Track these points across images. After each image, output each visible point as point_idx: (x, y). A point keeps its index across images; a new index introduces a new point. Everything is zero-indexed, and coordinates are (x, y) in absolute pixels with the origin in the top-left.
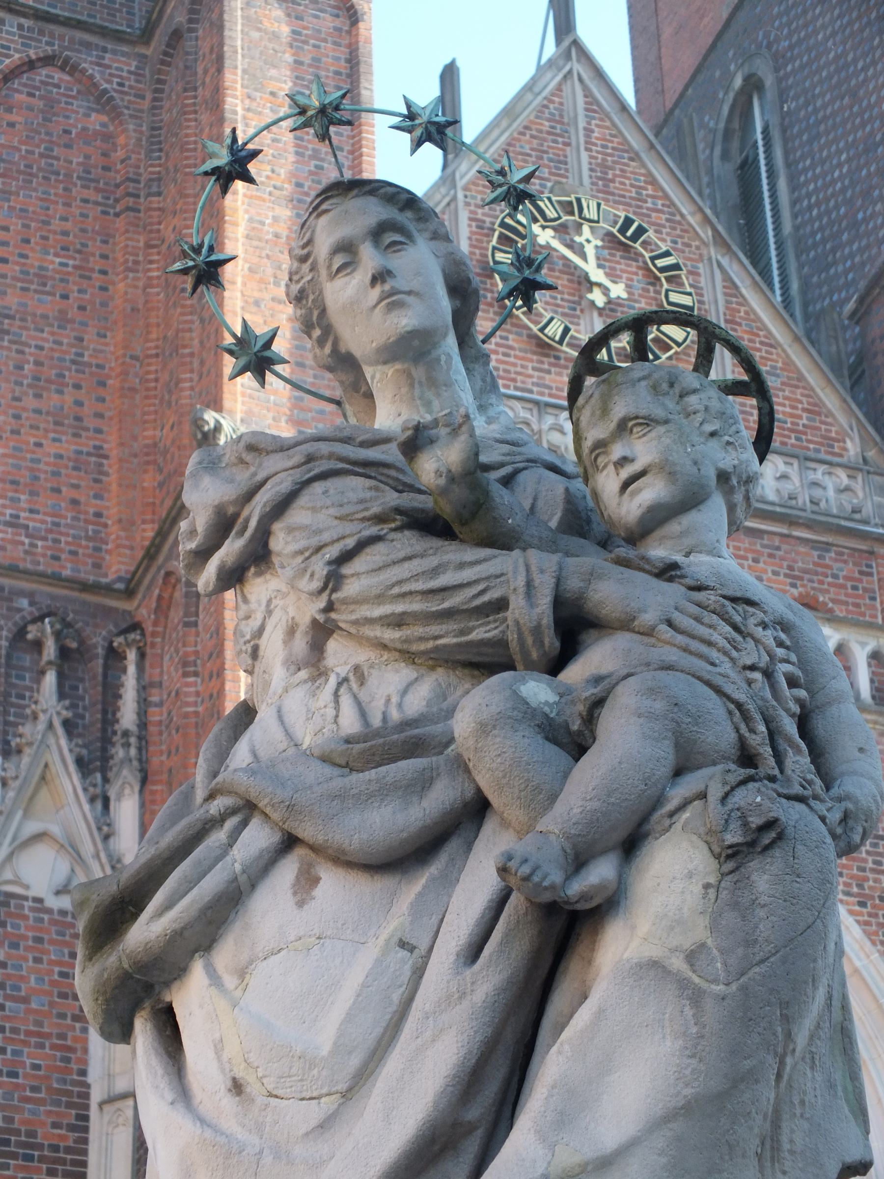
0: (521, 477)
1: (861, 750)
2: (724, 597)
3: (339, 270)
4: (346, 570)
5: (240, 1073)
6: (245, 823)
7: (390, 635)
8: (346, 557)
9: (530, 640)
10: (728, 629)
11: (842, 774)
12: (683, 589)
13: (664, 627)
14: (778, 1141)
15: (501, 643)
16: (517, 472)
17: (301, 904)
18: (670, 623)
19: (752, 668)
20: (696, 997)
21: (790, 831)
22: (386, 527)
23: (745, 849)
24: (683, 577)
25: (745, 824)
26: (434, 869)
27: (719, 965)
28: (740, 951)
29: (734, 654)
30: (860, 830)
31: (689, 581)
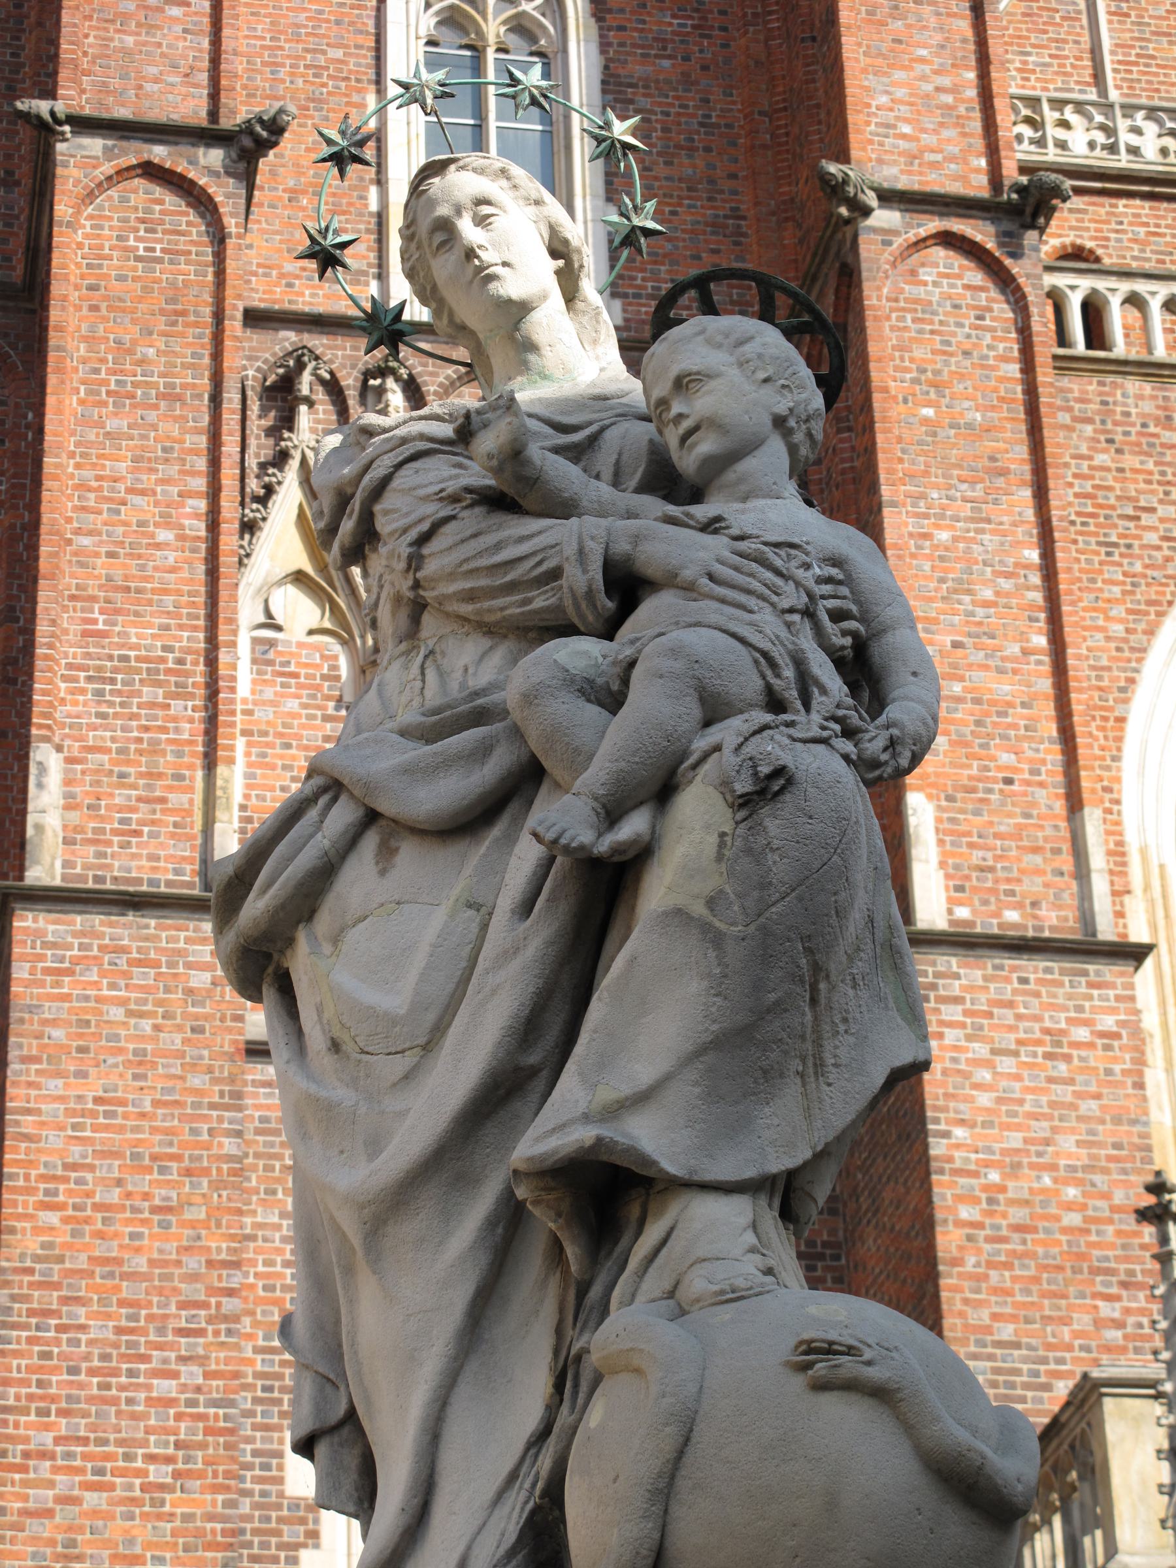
0: (608, 434)
1: (915, 674)
2: (766, 544)
3: (438, 249)
4: (426, 551)
5: (337, 1033)
6: (335, 800)
7: (466, 609)
8: (424, 539)
9: (584, 605)
10: (769, 575)
11: (894, 700)
12: (726, 540)
13: (705, 581)
14: (821, 1059)
15: (559, 609)
16: (603, 429)
17: (383, 872)
18: (711, 577)
19: (791, 611)
20: (717, 940)
21: (800, 776)
22: (458, 505)
23: (755, 797)
24: (727, 528)
25: (756, 774)
26: (496, 831)
27: (736, 908)
28: (756, 894)
29: (774, 598)
30: (908, 754)
31: (735, 531)
